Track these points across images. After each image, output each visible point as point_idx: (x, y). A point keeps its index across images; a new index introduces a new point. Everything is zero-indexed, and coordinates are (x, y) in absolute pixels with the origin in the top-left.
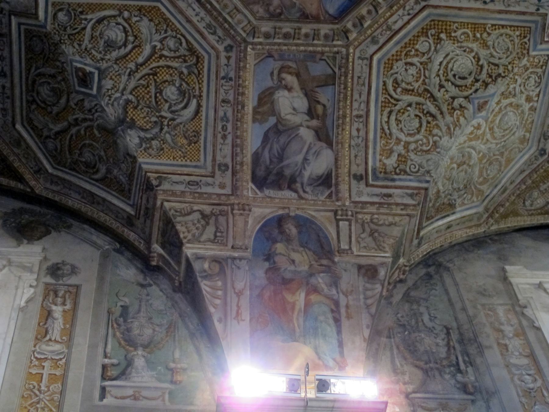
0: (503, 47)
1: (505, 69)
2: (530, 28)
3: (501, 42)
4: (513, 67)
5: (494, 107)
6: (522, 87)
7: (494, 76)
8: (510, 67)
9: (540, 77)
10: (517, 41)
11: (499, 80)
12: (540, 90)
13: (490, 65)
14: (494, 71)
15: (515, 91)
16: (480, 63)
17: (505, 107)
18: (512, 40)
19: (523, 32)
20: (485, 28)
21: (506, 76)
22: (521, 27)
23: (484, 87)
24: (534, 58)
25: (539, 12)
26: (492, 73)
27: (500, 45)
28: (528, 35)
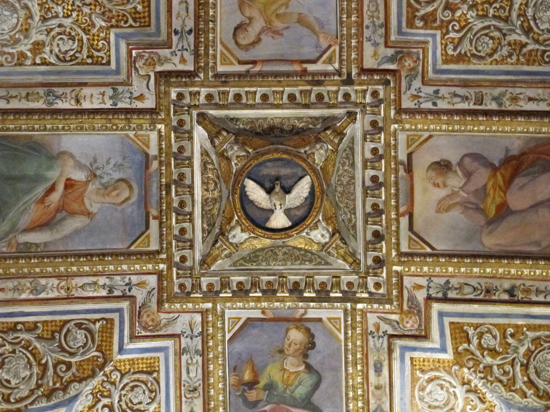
2: (149, 26)
6: (58, 30)
9: (74, 58)
12: (53, 64)
15: (53, 17)
19: (142, 15)
22: (149, 11)
24: (105, 39)
25: (173, 34)
28: (138, 24)
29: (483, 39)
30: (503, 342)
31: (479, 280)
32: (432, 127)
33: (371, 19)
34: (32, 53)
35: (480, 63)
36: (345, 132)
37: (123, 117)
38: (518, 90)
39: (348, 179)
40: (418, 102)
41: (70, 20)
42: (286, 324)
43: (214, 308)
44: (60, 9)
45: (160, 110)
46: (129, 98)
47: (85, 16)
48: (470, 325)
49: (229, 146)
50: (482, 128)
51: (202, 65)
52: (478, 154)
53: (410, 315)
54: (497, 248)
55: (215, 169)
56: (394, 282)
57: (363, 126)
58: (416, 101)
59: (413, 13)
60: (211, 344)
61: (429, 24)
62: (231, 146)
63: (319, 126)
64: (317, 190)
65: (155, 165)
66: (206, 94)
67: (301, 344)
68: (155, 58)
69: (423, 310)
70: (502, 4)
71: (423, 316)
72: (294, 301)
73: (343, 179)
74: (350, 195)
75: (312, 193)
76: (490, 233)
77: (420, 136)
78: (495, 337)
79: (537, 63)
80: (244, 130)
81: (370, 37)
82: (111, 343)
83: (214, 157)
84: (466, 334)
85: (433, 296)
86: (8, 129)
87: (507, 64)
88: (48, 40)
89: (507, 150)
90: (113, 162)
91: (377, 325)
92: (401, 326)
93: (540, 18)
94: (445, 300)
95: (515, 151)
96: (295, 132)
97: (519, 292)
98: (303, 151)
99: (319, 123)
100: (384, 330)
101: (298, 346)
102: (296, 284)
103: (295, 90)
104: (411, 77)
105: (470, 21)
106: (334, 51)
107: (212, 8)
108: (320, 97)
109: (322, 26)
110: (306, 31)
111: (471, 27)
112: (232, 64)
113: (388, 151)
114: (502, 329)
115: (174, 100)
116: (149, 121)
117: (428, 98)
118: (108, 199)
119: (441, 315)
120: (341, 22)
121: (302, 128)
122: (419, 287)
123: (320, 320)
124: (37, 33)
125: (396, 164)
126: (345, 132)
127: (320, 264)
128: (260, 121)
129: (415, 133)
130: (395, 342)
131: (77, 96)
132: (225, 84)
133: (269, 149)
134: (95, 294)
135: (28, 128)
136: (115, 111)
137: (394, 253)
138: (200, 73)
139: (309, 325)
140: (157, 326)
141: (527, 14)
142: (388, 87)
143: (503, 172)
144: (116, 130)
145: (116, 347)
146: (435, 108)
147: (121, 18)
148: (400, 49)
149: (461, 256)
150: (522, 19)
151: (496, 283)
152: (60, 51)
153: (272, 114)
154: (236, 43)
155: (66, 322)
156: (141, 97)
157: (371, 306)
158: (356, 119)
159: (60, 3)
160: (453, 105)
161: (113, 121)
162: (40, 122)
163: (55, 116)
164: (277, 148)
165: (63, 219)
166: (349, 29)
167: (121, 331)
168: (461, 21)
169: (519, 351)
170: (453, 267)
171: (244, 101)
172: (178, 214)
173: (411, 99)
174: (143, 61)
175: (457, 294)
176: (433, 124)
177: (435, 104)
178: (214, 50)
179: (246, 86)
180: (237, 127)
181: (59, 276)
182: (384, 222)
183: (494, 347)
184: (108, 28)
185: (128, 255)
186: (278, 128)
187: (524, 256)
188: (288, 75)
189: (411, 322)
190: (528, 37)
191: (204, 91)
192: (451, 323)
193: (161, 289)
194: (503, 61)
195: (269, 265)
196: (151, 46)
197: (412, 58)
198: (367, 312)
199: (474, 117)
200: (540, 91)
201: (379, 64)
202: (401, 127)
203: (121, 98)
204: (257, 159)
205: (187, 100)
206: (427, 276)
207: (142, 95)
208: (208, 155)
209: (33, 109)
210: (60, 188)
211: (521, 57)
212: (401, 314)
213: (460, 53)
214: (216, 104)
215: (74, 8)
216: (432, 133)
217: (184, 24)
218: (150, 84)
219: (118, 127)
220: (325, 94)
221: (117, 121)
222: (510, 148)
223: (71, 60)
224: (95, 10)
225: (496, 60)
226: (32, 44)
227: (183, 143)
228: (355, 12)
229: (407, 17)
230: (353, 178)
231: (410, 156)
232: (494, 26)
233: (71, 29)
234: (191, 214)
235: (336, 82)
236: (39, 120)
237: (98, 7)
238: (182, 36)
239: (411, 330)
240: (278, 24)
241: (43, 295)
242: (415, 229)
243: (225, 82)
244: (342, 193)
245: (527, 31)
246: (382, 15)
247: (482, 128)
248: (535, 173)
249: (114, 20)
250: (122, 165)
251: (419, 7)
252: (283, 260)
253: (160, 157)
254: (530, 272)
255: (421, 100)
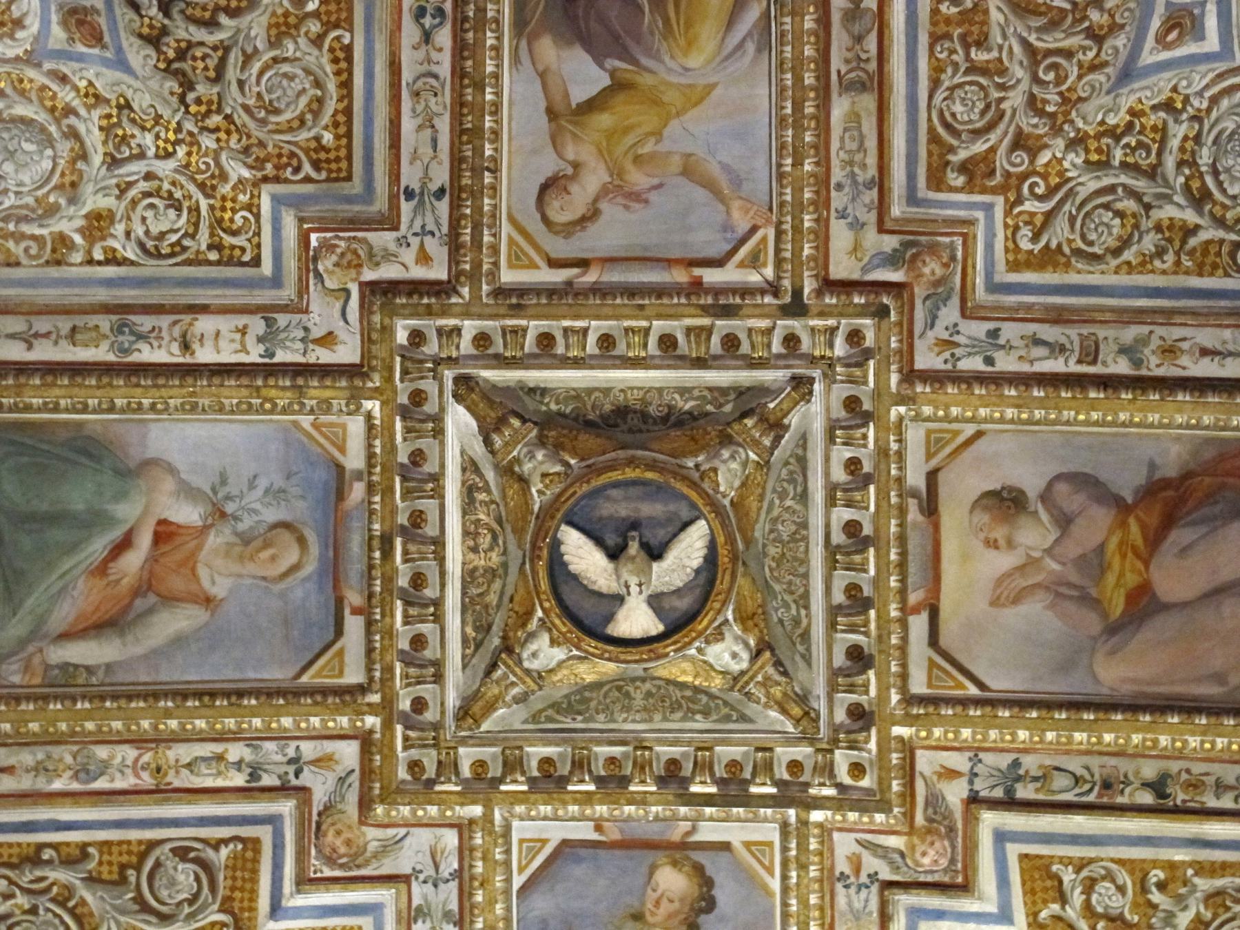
0: (279, 93)
1: (210, 102)
2: (349, 178)
3: (297, 85)
4: (217, 130)
5: (76, 80)
6: (143, 186)
7: (186, 66)
8: (216, 120)
10: (303, 135)
11: (172, 85)
12: (132, 263)
13: (220, 53)
14: (200, 65)
15: (132, 158)
16: (223, 19)
17: (73, 134)
18: (302, 122)
19: (332, 155)
20: (337, 26)
21: (187, 107)
22: (349, 147)
23: (146, 31)
24: (249, 207)
25: (402, 197)
26: (194, 59)
27: (285, 82)
28: (324, 175)
29: (1100, 216)
30: (1141, 900)
31: (1086, 760)
32: (983, 412)
33: (848, 169)
34: (84, 237)
35: (1091, 269)
36: (786, 421)
37: (288, 383)
38: (1177, 332)
39: (793, 528)
40: (953, 355)
41: (171, 164)
42: (650, 856)
43: (488, 818)
44: (148, 139)
45: (372, 369)
46: (302, 340)
47: (206, 155)
48: (1066, 861)
49: (525, 450)
50: (1095, 416)
51: (467, 267)
52: (1085, 474)
53: (929, 839)
54: (1127, 689)
55: (493, 502)
56: (894, 762)
57: (828, 410)
58: (947, 355)
59: (942, 156)
60: (479, 897)
61: (978, 181)
62: (530, 452)
63: (728, 408)
64: (723, 552)
65: (358, 491)
66: (474, 332)
67: (682, 900)
68: (361, 252)
69: (960, 825)
70: (1142, 138)
71: (960, 840)
72: (668, 803)
73: (780, 527)
74: (796, 564)
75: (711, 559)
76: (1112, 653)
77: (956, 433)
78: (1121, 889)
79: (1220, 271)
80: (560, 414)
81: (846, 209)
82: (254, 893)
83: (490, 475)
84: (1056, 883)
85: (982, 794)
86: (28, 408)
87: (1153, 271)
88: (120, 208)
89: (1152, 466)
90: (263, 483)
91: (855, 859)
92: (909, 862)
93: (1228, 170)
94: (1010, 803)
95: (1171, 472)
96: (674, 420)
97: (1178, 787)
98: (691, 464)
99: (728, 402)
100: (872, 872)
101: (677, 905)
102: (673, 764)
103: (675, 327)
104: (937, 299)
105: (1070, 174)
106: (764, 239)
107: (492, 142)
108: (731, 342)
109: (737, 182)
110: (700, 194)
111: (1071, 189)
112: (533, 266)
113: (883, 466)
114: (1139, 870)
115: (402, 346)
116: (347, 393)
117: (974, 346)
118: (251, 568)
119: (1001, 837)
120: (781, 176)
121: (690, 413)
122: (951, 774)
123: (726, 846)
124: (97, 192)
125: (900, 496)
126: (786, 421)
127: (727, 719)
128: (597, 394)
129: (945, 426)
130: (896, 898)
131: (184, 336)
132: (517, 311)
133: (615, 460)
134: (220, 783)
135: (73, 405)
136: (271, 370)
137: (895, 697)
138: (463, 285)
139: (698, 857)
140: (358, 855)
141: (1200, 162)
142: (885, 324)
143: (1141, 514)
144: (272, 412)
145: (264, 903)
146: (990, 369)
147: (285, 160)
148: (911, 237)
149: (1048, 705)
150: (1187, 171)
151: (1124, 766)
152: (147, 233)
153: (623, 380)
154: (545, 220)
155: (153, 845)
156: (328, 340)
157: (843, 816)
158: (811, 393)
159: (148, 126)
160: (1032, 362)
161: (264, 392)
162: (99, 393)
163: (134, 380)
164: (633, 457)
165: (150, 611)
166: (798, 191)
167: (277, 867)
168: (1049, 174)
169: (1177, 921)
170: (1027, 729)
171: (560, 350)
172: (408, 603)
173: (936, 349)
174: (334, 258)
175: (1037, 790)
176: (986, 406)
177: (989, 361)
178: (494, 235)
179: (564, 317)
180: (544, 408)
181: (138, 741)
182: (873, 626)
183: (1119, 911)
184: (256, 184)
185: (292, 694)
186: (635, 412)
187: (1189, 707)
188: (659, 291)
189: (932, 852)
190: (1200, 212)
191: (470, 327)
192: (1024, 857)
193: (367, 772)
194: (1144, 264)
195: (614, 721)
196: (354, 223)
197: (940, 257)
198: (832, 830)
199: (1078, 390)
200: (1227, 334)
201: (865, 270)
202: (913, 413)
203: (283, 341)
204: (588, 482)
205: (432, 347)
206: (969, 749)
207: (330, 333)
208: (477, 470)
209: (86, 364)
210: (144, 540)
211: (1184, 258)
212: (909, 834)
213: (1047, 246)
214: (497, 356)
215: (180, 136)
216: (984, 426)
217: (426, 176)
218: (348, 310)
219: (275, 405)
220: (743, 336)
221: (273, 393)
222: (1158, 461)
223: (172, 255)
224: (227, 141)
225: (1128, 263)
226: (86, 216)
227: (422, 443)
228: (812, 152)
229: (929, 165)
230: (804, 525)
231: (932, 476)
232: (1124, 186)
233: (173, 184)
234: (438, 603)
235: (767, 310)
236: (99, 387)
237: (235, 137)
238: (421, 203)
239: (932, 872)
240: (638, 179)
241: (101, 784)
242: (944, 642)
243: (518, 306)
244: (779, 560)
245: (1199, 199)
246: (872, 160)
247: (1095, 416)
248: (1215, 518)
249: (269, 166)
250: (284, 491)
251: (955, 142)
252: (645, 709)
253: (370, 473)
254: (1202, 742)
255: (958, 352)
